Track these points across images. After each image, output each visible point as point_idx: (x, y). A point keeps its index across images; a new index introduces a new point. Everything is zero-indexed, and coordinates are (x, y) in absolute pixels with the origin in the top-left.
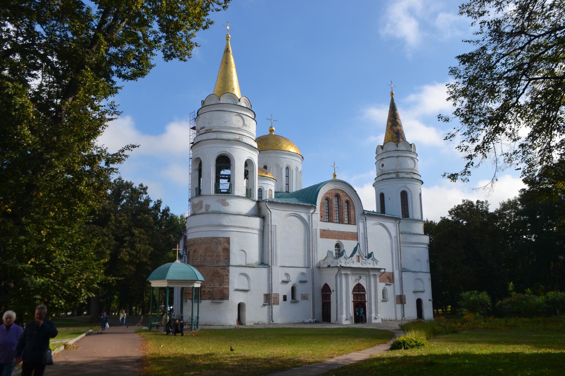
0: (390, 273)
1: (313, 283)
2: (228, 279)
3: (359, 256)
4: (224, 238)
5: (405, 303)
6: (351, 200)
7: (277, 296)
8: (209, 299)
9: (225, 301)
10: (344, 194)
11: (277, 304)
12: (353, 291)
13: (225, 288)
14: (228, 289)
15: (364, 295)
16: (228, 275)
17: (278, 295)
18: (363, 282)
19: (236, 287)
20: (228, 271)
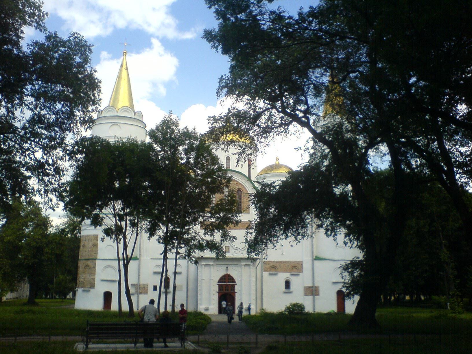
0: (298, 263)
1: (188, 274)
2: (95, 271)
3: (229, 246)
4: (94, 235)
5: (318, 295)
6: (245, 188)
7: (146, 286)
8: (82, 287)
9: (91, 290)
10: (235, 182)
11: (146, 293)
12: (218, 282)
13: (92, 279)
14: (94, 280)
15: (233, 287)
16: (95, 268)
17: (147, 285)
18: (233, 272)
19: (101, 279)
20: (95, 264)
